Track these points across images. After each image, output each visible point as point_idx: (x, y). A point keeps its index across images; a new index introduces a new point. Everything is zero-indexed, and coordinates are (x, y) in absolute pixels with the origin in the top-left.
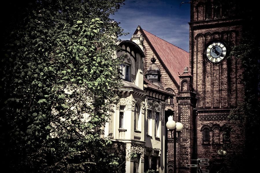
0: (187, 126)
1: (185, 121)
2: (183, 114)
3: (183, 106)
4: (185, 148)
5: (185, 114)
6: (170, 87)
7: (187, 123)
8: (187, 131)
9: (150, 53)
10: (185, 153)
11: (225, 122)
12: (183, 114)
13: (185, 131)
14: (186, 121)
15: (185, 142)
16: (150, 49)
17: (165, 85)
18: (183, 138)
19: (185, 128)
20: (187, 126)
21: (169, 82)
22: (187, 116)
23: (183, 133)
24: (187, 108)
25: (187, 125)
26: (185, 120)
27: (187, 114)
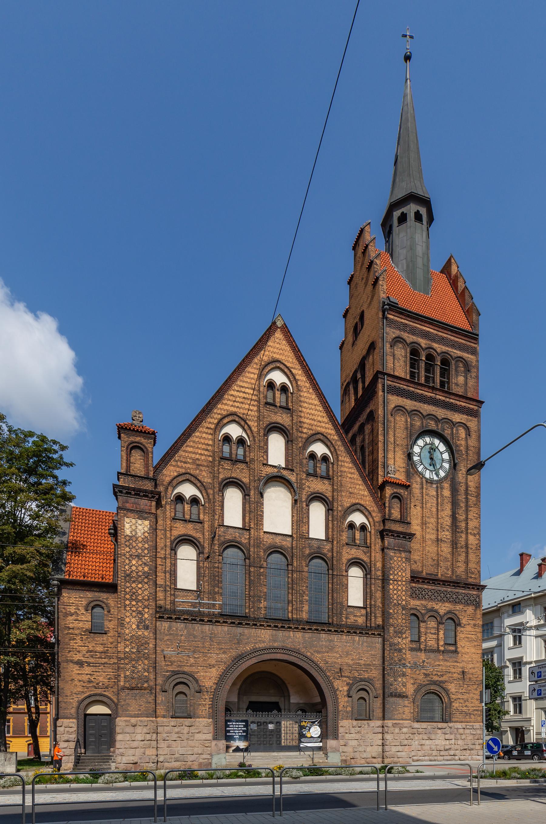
0: (403, 600)
1: (400, 588)
2: (396, 573)
3: (395, 553)
4: (400, 650)
5: (400, 574)
6: (362, 502)
7: (404, 593)
8: (404, 612)
9: (310, 401)
10: (400, 660)
11: (448, 607)
12: (396, 573)
13: (400, 612)
14: (402, 589)
15: (399, 638)
16: (311, 391)
17: (351, 493)
18: (394, 628)
19: (399, 604)
20: (403, 600)
21: (360, 490)
22: (404, 579)
23: (395, 616)
24: (404, 560)
25: (404, 598)
26: (400, 585)
27: (404, 574)
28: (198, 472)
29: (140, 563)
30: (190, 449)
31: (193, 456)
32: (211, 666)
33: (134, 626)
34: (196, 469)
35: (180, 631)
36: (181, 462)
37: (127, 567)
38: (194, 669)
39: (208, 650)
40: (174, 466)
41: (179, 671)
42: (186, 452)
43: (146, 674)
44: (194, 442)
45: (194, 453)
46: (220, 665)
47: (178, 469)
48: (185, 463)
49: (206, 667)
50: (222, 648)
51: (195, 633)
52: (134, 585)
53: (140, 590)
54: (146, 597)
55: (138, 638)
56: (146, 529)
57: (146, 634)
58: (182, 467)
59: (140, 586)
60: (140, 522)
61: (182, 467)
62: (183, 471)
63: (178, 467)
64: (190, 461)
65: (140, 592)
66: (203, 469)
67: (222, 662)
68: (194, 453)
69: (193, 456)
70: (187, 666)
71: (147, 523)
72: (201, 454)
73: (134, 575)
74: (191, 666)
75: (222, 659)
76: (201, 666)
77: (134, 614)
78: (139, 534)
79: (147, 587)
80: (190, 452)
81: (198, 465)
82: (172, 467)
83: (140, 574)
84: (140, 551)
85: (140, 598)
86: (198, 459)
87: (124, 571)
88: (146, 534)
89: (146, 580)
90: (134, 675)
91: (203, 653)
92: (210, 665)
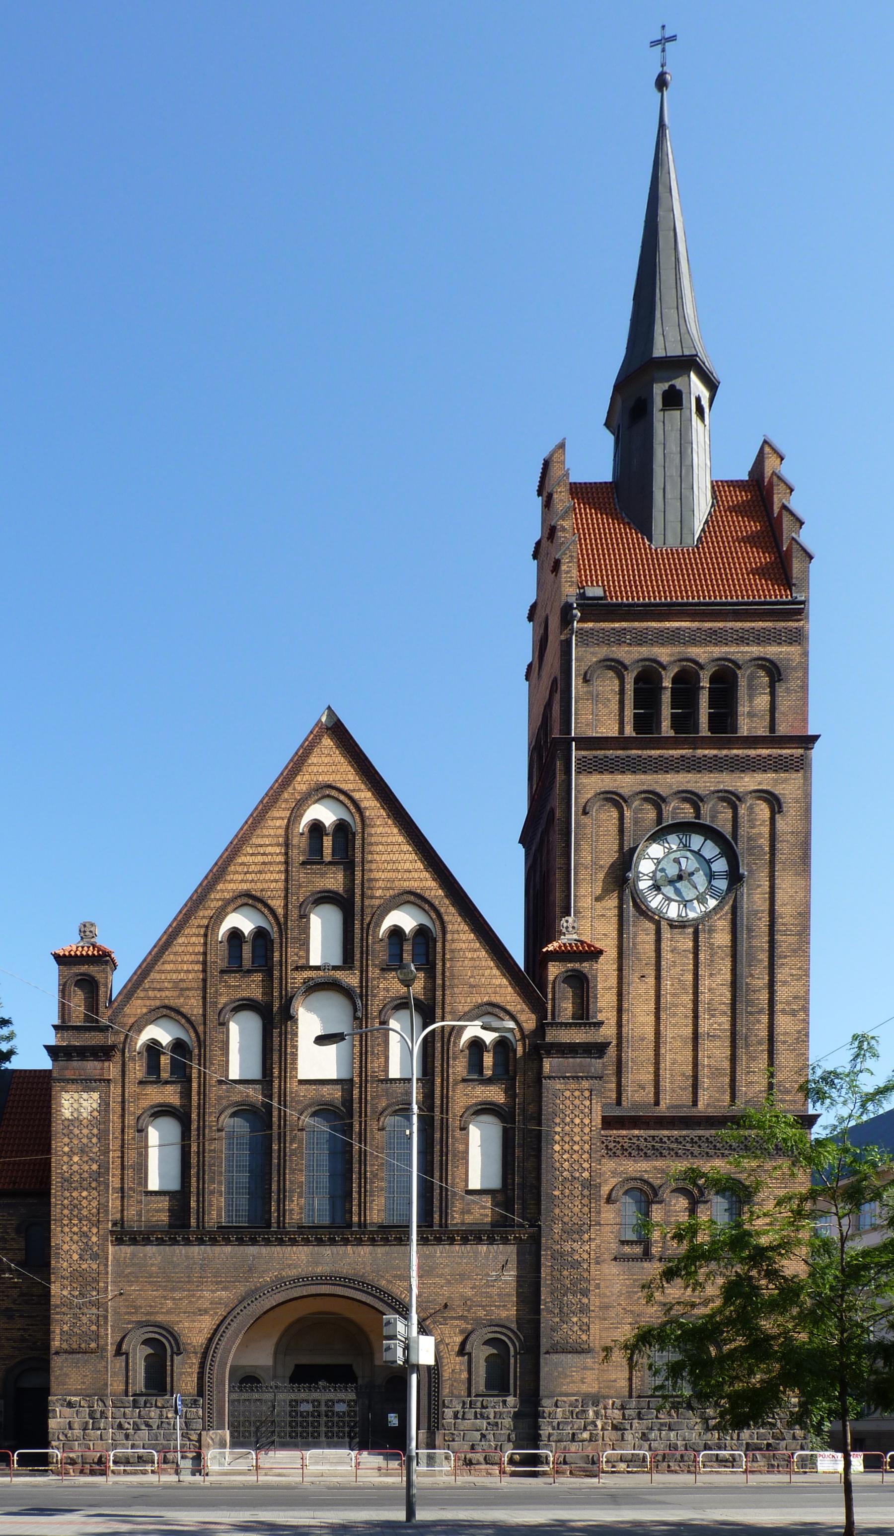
28: (182, 1000)
29: (85, 1159)
30: (168, 967)
31: (174, 976)
32: (204, 1312)
33: (76, 1257)
34: (179, 997)
35: (151, 1258)
36: (154, 989)
37: (64, 1168)
38: (173, 1318)
39: (198, 1286)
40: (142, 999)
41: (149, 1321)
42: (163, 972)
43: (94, 1328)
44: (175, 954)
45: (175, 972)
46: (218, 1308)
47: (148, 1003)
48: (160, 990)
49: (193, 1313)
50: (221, 1282)
51: (175, 1259)
52: (75, 1194)
53: (84, 1201)
54: (95, 1210)
55: (82, 1274)
56: (95, 1106)
57: (95, 1267)
58: (155, 998)
59: (85, 1194)
60: (85, 1095)
61: (155, 998)
62: (158, 1003)
63: (149, 998)
64: (169, 986)
65: (85, 1203)
66: (191, 995)
67: (220, 1304)
68: (175, 972)
69: (174, 976)
70: (162, 1313)
71: (96, 1095)
72: (188, 971)
73: (76, 1178)
74: (168, 1312)
75: (221, 1299)
76: (185, 1313)
77: (75, 1238)
78: (85, 1115)
79: (96, 1194)
80: (169, 972)
81: (182, 989)
82: (139, 1001)
83: (86, 1175)
84: (85, 1141)
85: (85, 1212)
86: (182, 980)
87: (60, 1173)
88: (96, 1114)
89: (94, 1185)
90: (75, 1330)
91: (189, 1291)
92: (200, 1311)
